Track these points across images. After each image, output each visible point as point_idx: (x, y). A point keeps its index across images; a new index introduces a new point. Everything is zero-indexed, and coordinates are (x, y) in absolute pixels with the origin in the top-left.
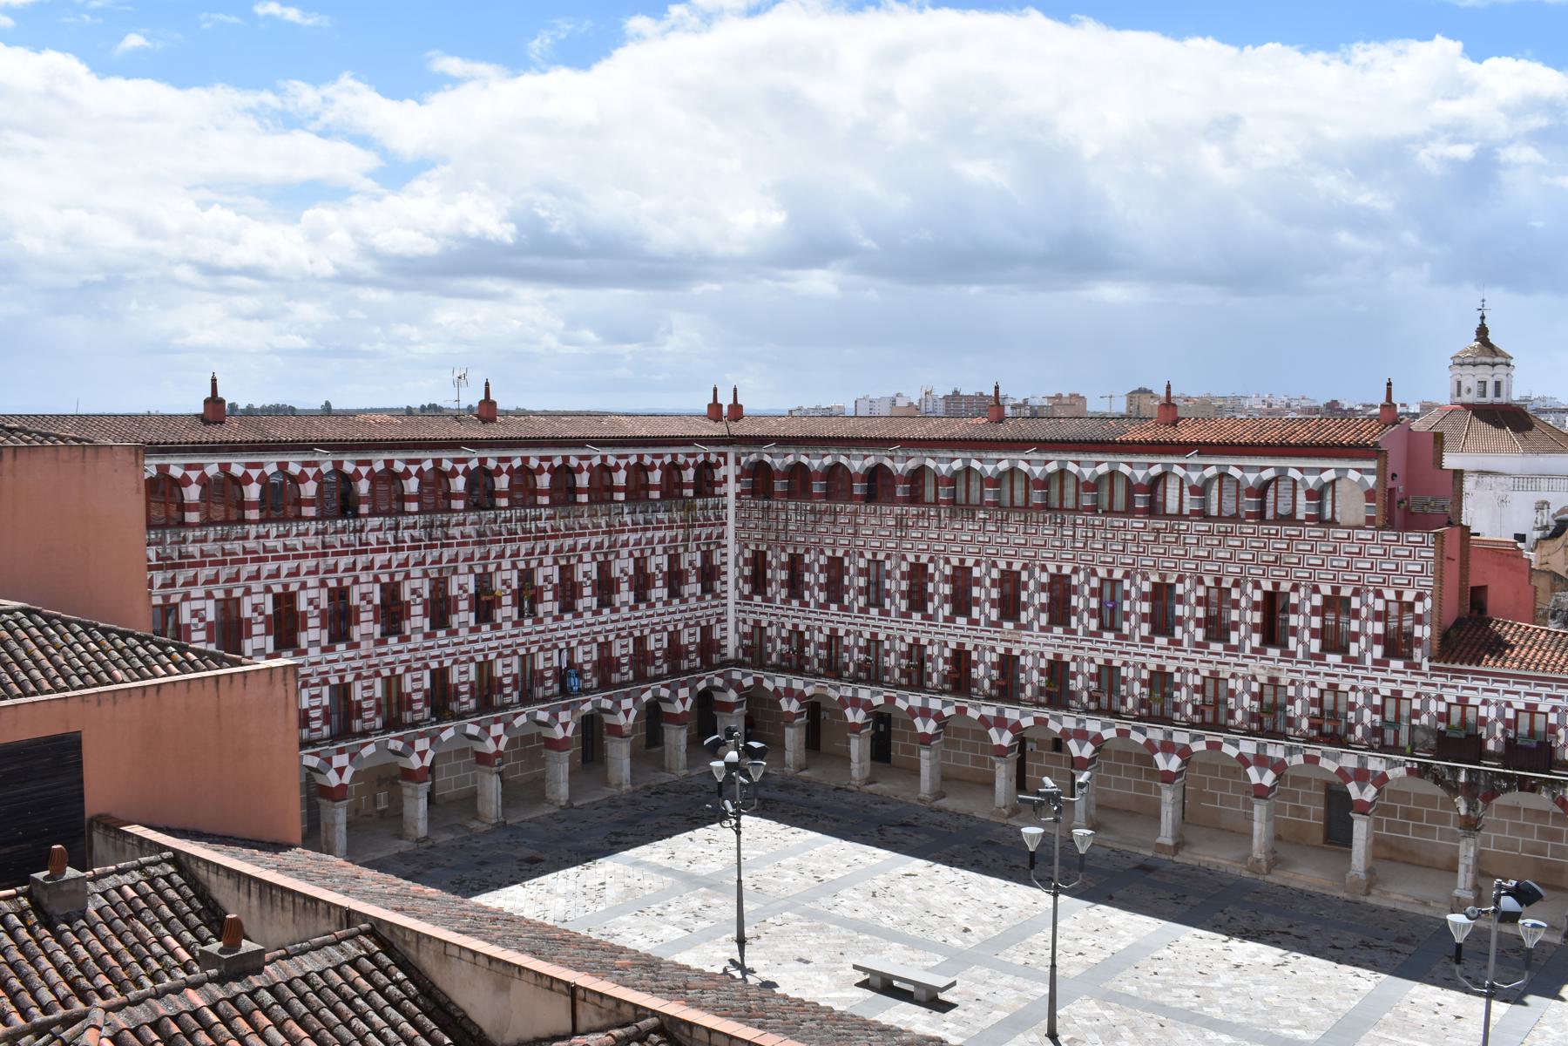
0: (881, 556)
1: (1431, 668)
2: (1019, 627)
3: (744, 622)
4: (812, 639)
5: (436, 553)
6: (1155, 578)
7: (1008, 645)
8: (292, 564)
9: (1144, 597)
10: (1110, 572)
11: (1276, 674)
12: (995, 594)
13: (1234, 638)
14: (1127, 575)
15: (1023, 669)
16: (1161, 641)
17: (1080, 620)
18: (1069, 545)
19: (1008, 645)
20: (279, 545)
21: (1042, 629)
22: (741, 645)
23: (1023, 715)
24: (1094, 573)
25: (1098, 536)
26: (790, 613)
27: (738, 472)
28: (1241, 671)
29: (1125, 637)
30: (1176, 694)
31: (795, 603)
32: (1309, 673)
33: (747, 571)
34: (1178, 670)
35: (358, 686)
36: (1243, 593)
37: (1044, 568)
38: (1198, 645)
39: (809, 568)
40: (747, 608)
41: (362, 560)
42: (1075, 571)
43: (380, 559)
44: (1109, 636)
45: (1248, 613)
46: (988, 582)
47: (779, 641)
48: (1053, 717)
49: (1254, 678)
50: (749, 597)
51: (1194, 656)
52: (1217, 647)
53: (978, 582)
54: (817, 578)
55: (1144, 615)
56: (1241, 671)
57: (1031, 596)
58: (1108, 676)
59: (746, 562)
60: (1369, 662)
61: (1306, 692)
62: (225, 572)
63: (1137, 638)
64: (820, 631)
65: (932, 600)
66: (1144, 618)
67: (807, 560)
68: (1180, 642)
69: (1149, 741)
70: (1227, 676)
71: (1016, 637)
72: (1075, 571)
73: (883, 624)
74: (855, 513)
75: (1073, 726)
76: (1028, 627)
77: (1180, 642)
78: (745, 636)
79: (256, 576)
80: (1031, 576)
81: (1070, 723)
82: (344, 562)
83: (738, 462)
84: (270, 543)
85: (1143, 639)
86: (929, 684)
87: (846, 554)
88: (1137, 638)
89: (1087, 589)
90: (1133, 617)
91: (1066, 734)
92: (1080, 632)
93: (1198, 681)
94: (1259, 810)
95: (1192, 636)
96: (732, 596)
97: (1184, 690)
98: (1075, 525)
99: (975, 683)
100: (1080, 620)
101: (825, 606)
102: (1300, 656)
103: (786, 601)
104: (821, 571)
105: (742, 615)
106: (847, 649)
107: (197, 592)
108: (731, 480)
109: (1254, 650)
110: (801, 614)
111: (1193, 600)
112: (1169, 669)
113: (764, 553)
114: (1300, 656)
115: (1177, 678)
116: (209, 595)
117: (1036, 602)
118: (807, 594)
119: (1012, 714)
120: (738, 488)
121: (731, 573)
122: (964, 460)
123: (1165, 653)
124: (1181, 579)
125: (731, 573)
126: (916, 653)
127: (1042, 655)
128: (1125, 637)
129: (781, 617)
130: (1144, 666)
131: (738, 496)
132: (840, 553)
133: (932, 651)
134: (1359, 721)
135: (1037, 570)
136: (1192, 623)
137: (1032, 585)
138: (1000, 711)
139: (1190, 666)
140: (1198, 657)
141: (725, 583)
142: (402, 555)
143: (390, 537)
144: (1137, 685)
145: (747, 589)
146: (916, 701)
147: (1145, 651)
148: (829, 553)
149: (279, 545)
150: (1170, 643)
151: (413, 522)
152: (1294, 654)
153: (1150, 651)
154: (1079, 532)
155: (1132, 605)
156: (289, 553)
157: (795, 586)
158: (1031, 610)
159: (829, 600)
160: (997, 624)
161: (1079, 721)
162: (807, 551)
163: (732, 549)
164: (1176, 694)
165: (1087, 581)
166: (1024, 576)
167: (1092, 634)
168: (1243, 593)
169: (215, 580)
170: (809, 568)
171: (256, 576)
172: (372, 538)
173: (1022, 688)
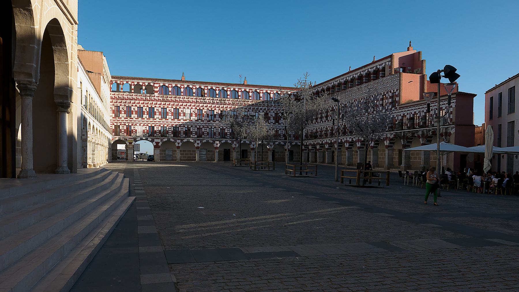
5: (222, 106)
8: (190, 104)
20: (187, 100)
35: (132, 127)
41: (205, 105)
43: (209, 105)
62: (176, 104)
79: (182, 105)
82: (201, 105)
84: (185, 100)
107: (170, 106)
116: (172, 107)
142: (214, 105)
143: (211, 101)
149: (187, 100)
151: (217, 100)
156: (189, 102)
169: (174, 105)
171: (182, 105)
172: (207, 101)
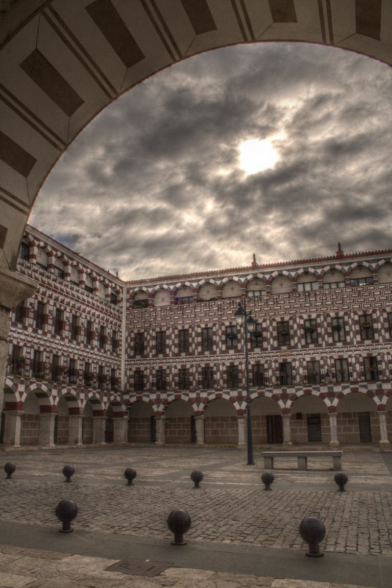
0: (210, 325)
2: (290, 347)
3: (130, 370)
4: (171, 372)
7: (284, 357)
10: (337, 314)
12: (275, 334)
14: (346, 314)
15: (294, 368)
19: (284, 357)
22: (128, 381)
26: (158, 361)
27: (128, 296)
29: (349, 344)
30: (379, 366)
31: (161, 356)
33: (132, 344)
37: (301, 317)
39: (169, 337)
40: (132, 362)
42: (318, 316)
44: (231, 352)
46: (271, 329)
47: (151, 377)
48: (315, 389)
50: (134, 357)
53: (266, 329)
54: (173, 341)
58: (184, 372)
59: (132, 340)
61: (329, 361)
63: (355, 343)
64: (175, 367)
65: (146, 349)
67: (168, 333)
68: (378, 341)
69: (369, 391)
71: (289, 353)
72: (318, 316)
73: (212, 358)
74: (195, 307)
76: (296, 346)
78: (131, 377)
80: (295, 321)
81: (324, 390)
83: (128, 292)
85: (358, 343)
86: (241, 385)
87: (190, 327)
88: (355, 343)
89: (325, 324)
90: (351, 333)
94: (333, 421)
96: (124, 357)
99: (267, 380)
101: (178, 355)
103: (155, 356)
104: (175, 337)
105: (129, 367)
106: (192, 374)
108: (124, 301)
110: (164, 361)
112: (374, 355)
113: (143, 334)
115: (379, 358)
118: (168, 350)
119: (290, 391)
120: (128, 304)
121: (124, 345)
122: (253, 274)
123: (371, 347)
125: (124, 345)
126: (184, 372)
128: (349, 344)
129: (151, 365)
131: (128, 309)
132: (187, 327)
133: (147, 372)
134: (354, 370)
135: (298, 319)
136: (383, 331)
138: (284, 390)
139: (385, 351)
141: (120, 350)
145: (132, 353)
146: (234, 394)
147: (360, 348)
148: (180, 328)
154: (318, 298)
155: (350, 327)
157: (161, 348)
158: (296, 339)
159: (180, 352)
160: (278, 348)
161: (329, 388)
162: (168, 329)
163: (124, 334)
164: (379, 366)
165: (220, 328)
166: (291, 323)
170: (169, 337)
173: (294, 378)
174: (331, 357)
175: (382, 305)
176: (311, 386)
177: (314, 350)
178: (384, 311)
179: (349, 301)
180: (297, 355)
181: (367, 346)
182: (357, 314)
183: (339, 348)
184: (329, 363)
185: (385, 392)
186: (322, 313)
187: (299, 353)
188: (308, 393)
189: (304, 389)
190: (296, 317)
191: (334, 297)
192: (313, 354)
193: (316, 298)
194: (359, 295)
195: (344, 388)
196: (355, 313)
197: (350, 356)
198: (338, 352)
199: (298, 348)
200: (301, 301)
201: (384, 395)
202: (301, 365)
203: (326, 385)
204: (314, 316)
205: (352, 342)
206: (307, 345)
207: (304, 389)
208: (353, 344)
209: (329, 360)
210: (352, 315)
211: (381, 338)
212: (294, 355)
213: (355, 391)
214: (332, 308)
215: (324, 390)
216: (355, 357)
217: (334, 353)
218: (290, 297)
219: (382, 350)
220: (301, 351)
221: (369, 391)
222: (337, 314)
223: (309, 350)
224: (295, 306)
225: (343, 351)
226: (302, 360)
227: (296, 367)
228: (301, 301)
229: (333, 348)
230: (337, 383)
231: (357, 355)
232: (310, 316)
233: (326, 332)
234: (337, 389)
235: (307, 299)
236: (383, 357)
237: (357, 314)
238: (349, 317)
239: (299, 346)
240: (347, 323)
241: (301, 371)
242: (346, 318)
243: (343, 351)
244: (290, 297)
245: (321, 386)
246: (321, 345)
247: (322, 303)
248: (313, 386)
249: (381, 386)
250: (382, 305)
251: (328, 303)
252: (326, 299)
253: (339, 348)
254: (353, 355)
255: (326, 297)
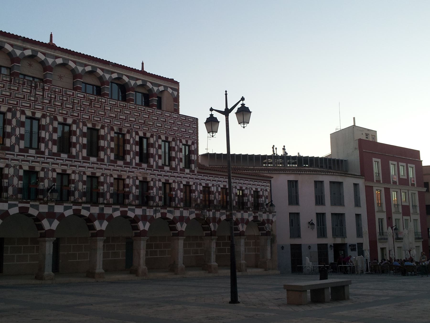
1: (198, 172)
6: (90, 125)
9: (84, 135)
10: (65, 119)
11: (146, 176)
13: (128, 158)
14: (74, 122)
16: (93, 159)
17: (47, 146)
18: (40, 100)
21: (21, 150)
23: (11, 206)
24: (55, 119)
25: (58, 98)
28: (131, 174)
29: (74, 157)
32: (158, 175)
34: (102, 175)
36: (131, 136)
37: (23, 112)
38: (112, 161)
42: (44, 116)
45: (134, 146)
48: (32, 206)
49: (137, 178)
51: (110, 167)
52: (120, 163)
55: (84, 145)
56: (131, 174)
57: (13, 129)
60: (179, 170)
63: (80, 158)
66: (84, 146)
68: (103, 160)
70: (125, 177)
72: (44, 116)
75: (46, 211)
77: (103, 160)
80: (14, 116)
85: (83, 158)
88: (80, 158)
90: (78, 146)
91: (41, 216)
92: (47, 153)
93: (112, 180)
95: (109, 157)
97: (105, 185)
98: (43, 89)
100: (47, 146)
102: (154, 167)
109: (136, 164)
111: (109, 138)
114: (154, 167)
117: (17, 133)
124: (103, 127)
127: (21, 167)
128: (74, 157)
130: (84, 173)
136: (109, 151)
137: (14, 122)
140: (112, 168)
144: (80, 184)
150: (98, 160)
152: (152, 166)
153: (88, 165)
154: (46, 94)
155: (77, 139)
158: (13, 138)
167: (54, 154)
168: (131, 136)
174: (54, 170)
175: (110, 123)
176: (29, 203)
177: (34, 157)
178: (112, 129)
179: (79, 108)
180: (12, 160)
181: (92, 163)
182: (86, 125)
183: (63, 160)
184: (50, 176)
185: (106, 217)
186: (48, 114)
187: (15, 158)
188: (24, 211)
189: (21, 205)
190: (17, 110)
191: (65, 99)
192: (32, 162)
193: (43, 94)
194: (91, 104)
195: (66, 208)
196: (85, 124)
197: (74, 172)
198: (62, 165)
199: (14, 151)
200: (24, 90)
201: (104, 219)
202: (16, 174)
203: (46, 203)
204: (38, 115)
205: (77, 156)
206: (25, 150)
207: (21, 205)
208: (78, 158)
209: (50, 173)
210: (81, 124)
211: (106, 156)
212: (8, 159)
213: (77, 213)
214: (61, 111)
215: (44, 209)
216: (79, 173)
217: (57, 166)
218: (11, 81)
219: (106, 171)
220: (17, 155)
221: (91, 215)
222: (65, 119)
223: (28, 156)
224: (17, 95)
225: (67, 165)
226: (18, 167)
227: (10, 176)
228: (24, 90)
229: (57, 159)
230: (60, 202)
231: (81, 172)
232: (34, 113)
233: (51, 139)
234: (59, 209)
235: (34, 91)
236: (105, 179)
237: (86, 125)
238: (78, 127)
239: (17, 148)
240: (75, 133)
241: (15, 180)
242: (74, 127)
243: (67, 165)
244: (11, 81)
245: (40, 204)
246: (43, 153)
247: (50, 102)
248: (31, 203)
249: (102, 209)
250: (110, 123)
251: (57, 103)
252: (55, 98)
253: (63, 160)
254: (77, 172)
255: (56, 96)
